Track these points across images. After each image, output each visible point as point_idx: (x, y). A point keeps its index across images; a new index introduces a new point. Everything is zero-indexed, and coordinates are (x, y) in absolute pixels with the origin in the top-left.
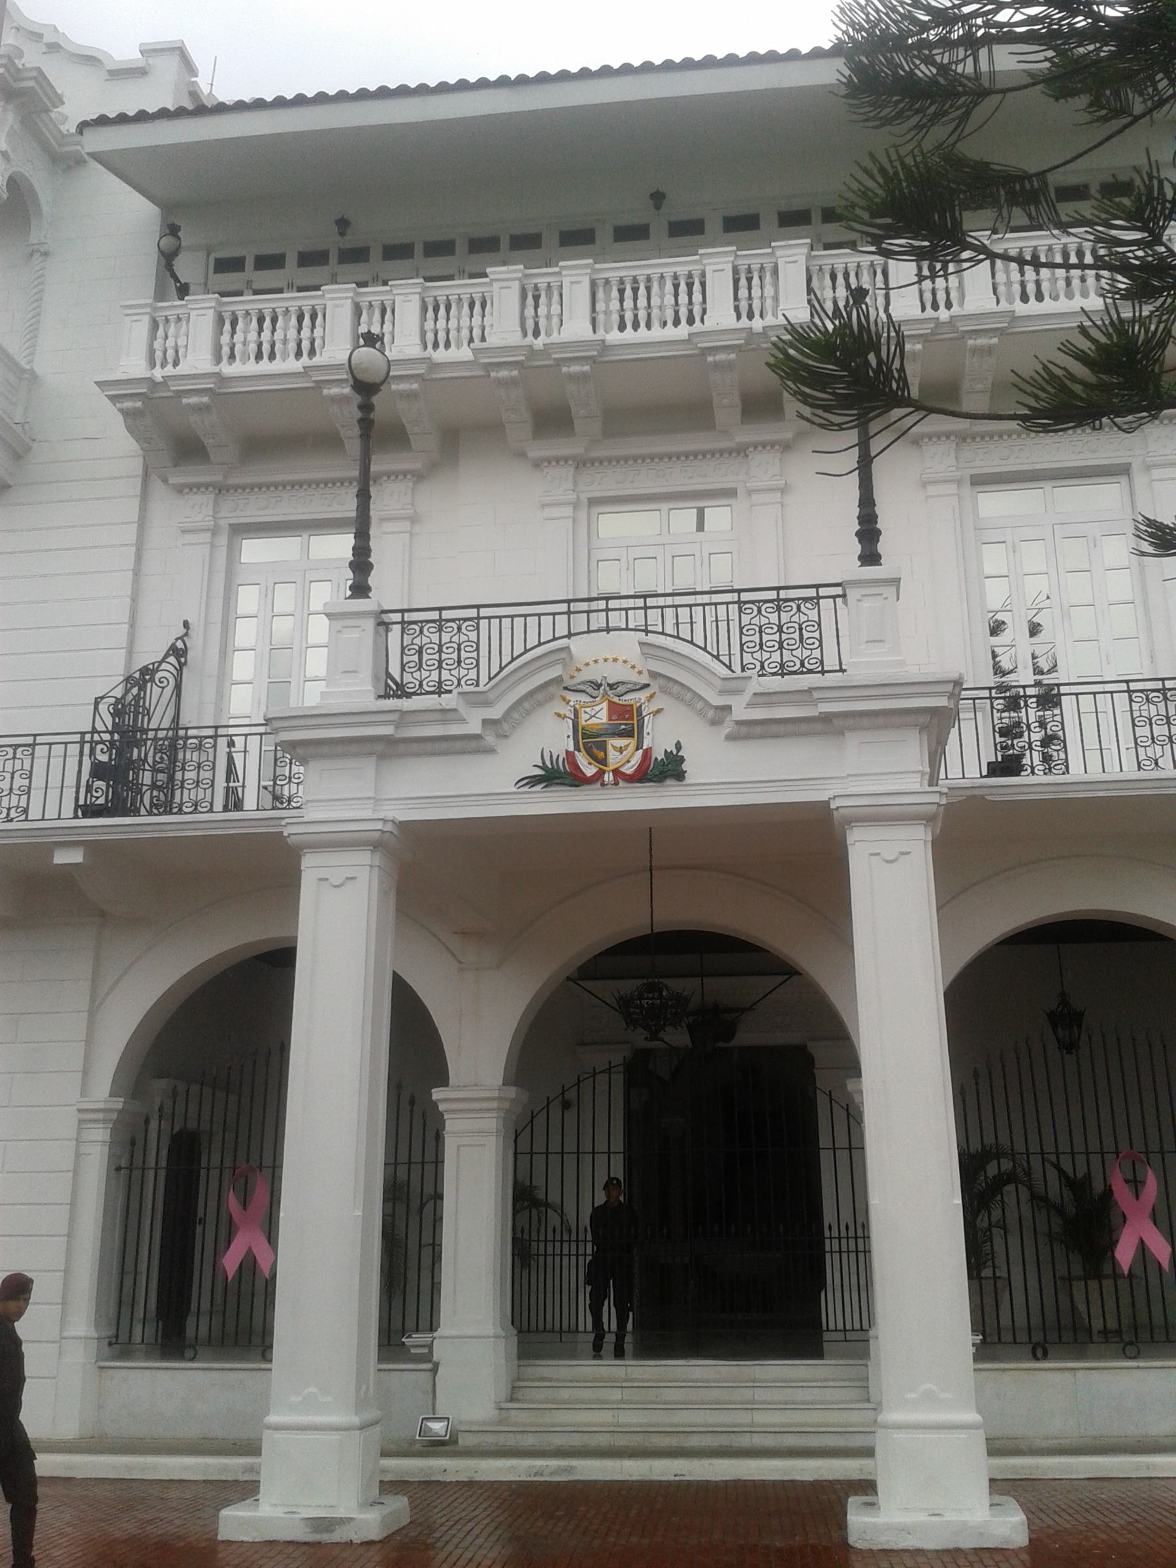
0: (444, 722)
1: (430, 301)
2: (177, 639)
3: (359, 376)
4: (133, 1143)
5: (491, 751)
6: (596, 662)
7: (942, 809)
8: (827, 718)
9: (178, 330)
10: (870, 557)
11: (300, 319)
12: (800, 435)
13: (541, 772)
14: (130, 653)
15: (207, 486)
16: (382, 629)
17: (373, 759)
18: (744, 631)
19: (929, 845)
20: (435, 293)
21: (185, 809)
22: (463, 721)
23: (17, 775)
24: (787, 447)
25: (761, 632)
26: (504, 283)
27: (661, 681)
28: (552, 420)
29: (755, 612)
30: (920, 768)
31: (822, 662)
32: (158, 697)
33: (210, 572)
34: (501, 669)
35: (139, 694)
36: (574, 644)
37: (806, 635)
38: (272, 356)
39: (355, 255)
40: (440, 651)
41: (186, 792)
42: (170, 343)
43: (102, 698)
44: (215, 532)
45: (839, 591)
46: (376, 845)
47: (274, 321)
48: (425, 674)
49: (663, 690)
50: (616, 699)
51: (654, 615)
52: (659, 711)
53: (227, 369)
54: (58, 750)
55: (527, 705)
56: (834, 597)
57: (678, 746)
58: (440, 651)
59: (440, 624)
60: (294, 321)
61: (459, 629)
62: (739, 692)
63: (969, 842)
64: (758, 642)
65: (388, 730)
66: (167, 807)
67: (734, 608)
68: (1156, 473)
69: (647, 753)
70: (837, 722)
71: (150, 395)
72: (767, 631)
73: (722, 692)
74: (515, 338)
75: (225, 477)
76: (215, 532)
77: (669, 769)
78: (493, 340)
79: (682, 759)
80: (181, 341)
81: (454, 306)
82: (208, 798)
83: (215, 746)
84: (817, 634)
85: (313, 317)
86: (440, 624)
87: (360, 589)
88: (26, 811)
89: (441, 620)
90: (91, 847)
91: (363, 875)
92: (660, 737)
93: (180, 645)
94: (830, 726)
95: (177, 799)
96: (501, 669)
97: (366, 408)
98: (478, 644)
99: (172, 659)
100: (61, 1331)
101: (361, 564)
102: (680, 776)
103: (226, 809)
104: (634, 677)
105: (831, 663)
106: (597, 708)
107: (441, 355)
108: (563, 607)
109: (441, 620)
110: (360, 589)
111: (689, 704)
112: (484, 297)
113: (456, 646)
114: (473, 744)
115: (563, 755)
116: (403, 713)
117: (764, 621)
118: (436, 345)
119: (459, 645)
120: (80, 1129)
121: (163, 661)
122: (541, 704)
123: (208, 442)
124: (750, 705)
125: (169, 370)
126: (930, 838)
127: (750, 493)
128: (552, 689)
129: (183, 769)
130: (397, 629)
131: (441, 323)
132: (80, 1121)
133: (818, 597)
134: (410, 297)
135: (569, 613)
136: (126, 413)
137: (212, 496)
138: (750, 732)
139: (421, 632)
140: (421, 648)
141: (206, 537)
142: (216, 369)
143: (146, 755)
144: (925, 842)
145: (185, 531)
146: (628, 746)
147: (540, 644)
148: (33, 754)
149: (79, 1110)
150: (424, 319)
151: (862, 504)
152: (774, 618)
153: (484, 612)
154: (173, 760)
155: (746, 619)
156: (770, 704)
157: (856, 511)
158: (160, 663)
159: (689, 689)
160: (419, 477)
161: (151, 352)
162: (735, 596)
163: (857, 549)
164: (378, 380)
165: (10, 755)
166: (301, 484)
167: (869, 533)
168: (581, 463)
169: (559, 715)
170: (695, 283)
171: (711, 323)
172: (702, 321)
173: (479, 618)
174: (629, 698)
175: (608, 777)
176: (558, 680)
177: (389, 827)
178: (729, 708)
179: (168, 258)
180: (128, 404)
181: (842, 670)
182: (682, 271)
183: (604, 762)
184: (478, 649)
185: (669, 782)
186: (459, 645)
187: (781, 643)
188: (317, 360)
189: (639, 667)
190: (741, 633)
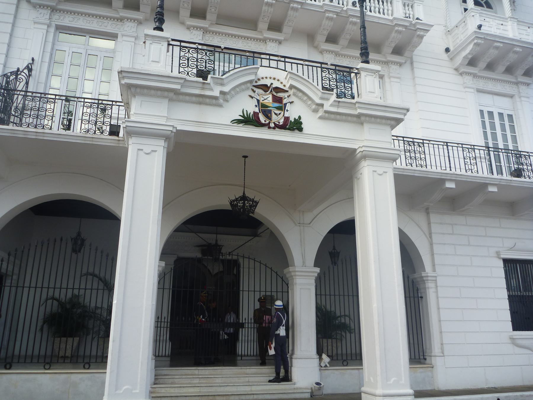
0: (203, 89)
5: (220, 106)
6: (266, 78)
8: (359, 116)
12: (286, 40)
14: (5, 66)
24: (280, 43)
25: (330, 80)
27: (293, 90)
33: (45, 41)
44: (49, 26)
46: (167, 138)
49: (294, 94)
50: (275, 94)
51: (288, 65)
55: (238, 89)
57: (300, 117)
58: (197, 61)
62: (328, 99)
65: (178, 87)
67: (319, 69)
68: (392, 79)
70: (363, 118)
73: (322, 98)
75: (56, 5)
79: (301, 123)
94: (359, 119)
99: (26, 71)
102: (300, 129)
104: (281, 86)
106: (265, 97)
111: (304, 102)
114: (214, 101)
115: (252, 113)
122: (243, 90)
124: (331, 105)
128: (249, 85)
130: (177, 49)
137: (50, 12)
138: (330, 116)
139: (189, 51)
145: (35, 23)
146: (280, 114)
152: (334, 76)
155: (324, 74)
156: (338, 107)
160: (140, 23)
162: (319, 65)
166: (89, 15)
174: (280, 95)
175: (272, 125)
176: (251, 82)
178: (322, 105)
183: (270, 118)
185: (297, 131)
187: (337, 86)
190: (322, 80)
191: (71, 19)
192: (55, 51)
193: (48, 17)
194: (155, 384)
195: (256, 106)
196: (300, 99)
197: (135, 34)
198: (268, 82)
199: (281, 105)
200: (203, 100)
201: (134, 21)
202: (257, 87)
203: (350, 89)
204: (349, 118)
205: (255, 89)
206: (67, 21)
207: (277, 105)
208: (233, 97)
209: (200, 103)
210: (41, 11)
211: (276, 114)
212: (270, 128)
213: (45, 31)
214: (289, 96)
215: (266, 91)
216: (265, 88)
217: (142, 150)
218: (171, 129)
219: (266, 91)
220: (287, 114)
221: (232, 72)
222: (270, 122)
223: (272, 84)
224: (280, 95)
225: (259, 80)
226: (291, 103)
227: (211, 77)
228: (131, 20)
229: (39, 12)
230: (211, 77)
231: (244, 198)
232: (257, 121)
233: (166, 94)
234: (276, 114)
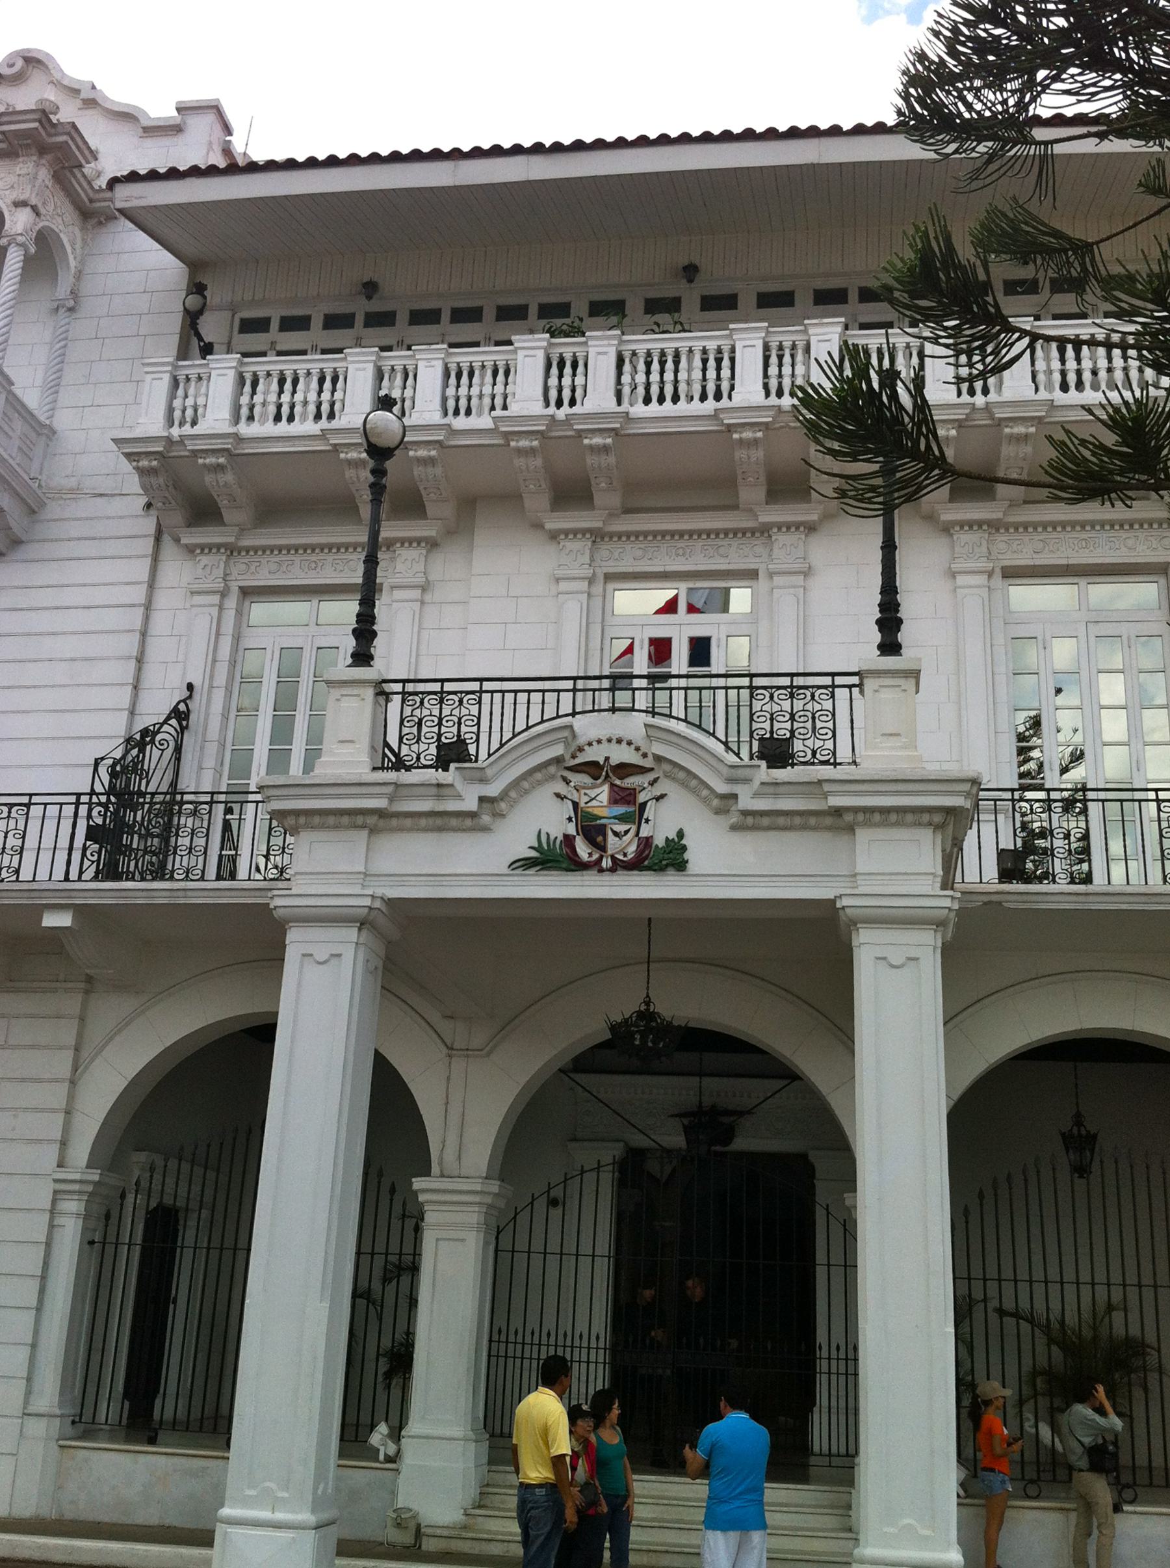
0: (439, 797)
1: (453, 368)
2: (178, 703)
3: (373, 440)
4: (108, 1217)
5: (486, 829)
6: (599, 742)
7: (952, 915)
8: (838, 812)
9: (197, 389)
10: (890, 647)
11: (322, 381)
12: (827, 517)
13: (534, 854)
14: (132, 713)
15: (219, 546)
16: (382, 699)
17: (365, 833)
18: (755, 717)
19: (939, 951)
20: (458, 359)
21: (176, 876)
22: (459, 797)
23: (10, 835)
24: (811, 528)
25: (772, 719)
26: (529, 353)
27: (666, 767)
28: (571, 492)
29: (767, 699)
30: (933, 871)
31: (834, 753)
32: (156, 758)
34: (502, 745)
35: (138, 756)
36: (578, 723)
37: (819, 724)
38: (291, 418)
39: (381, 319)
40: (440, 724)
41: (178, 858)
42: (190, 402)
43: (102, 759)
45: (855, 680)
46: (363, 923)
47: (295, 382)
48: (423, 747)
49: (667, 776)
50: (618, 782)
52: (662, 796)
53: (244, 429)
54: (53, 811)
56: (850, 687)
57: (681, 834)
58: (440, 724)
59: (441, 696)
60: (314, 385)
61: (461, 702)
62: (747, 781)
63: (978, 948)
64: (768, 729)
66: (160, 872)
67: (745, 693)
69: (648, 841)
70: (848, 818)
71: (166, 455)
72: (780, 718)
73: (731, 780)
74: (537, 408)
75: (237, 539)
76: (224, 594)
77: (670, 857)
78: (515, 409)
79: (684, 848)
80: (201, 401)
81: (477, 373)
82: (200, 866)
83: (210, 812)
84: (830, 725)
85: (335, 380)
86: (441, 696)
87: (362, 657)
88: (17, 872)
89: (442, 692)
90: (80, 911)
91: (349, 953)
92: (661, 825)
93: (182, 707)
94: (841, 822)
95: (170, 867)
96: (502, 745)
97: (379, 472)
98: (479, 719)
99: (173, 722)
100: (25, 1408)
101: (365, 631)
103: (219, 878)
105: (844, 754)
107: (461, 422)
108: (569, 684)
109: (442, 692)
110: (362, 657)
111: (694, 791)
112: (507, 365)
113: (456, 720)
114: (468, 822)
115: (560, 838)
116: (397, 785)
117: (776, 708)
118: (456, 412)
119: (460, 719)
120: (54, 1202)
121: (165, 722)
122: (540, 783)
123: (223, 503)
125: (187, 430)
126: (939, 944)
127: (771, 575)
128: (552, 769)
129: (177, 835)
131: (463, 391)
132: (55, 1192)
133: (834, 686)
134: (434, 363)
135: (574, 690)
136: (141, 471)
139: (422, 703)
140: (420, 720)
141: (216, 599)
142: (232, 430)
143: (143, 818)
144: (935, 948)
146: (627, 832)
147: (543, 721)
148: (27, 814)
149: (55, 1181)
150: (446, 385)
151: (883, 592)
152: (786, 705)
153: (487, 686)
154: (168, 826)
156: (776, 795)
157: (878, 598)
158: (162, 725)
159: (696, 777)
160: (432, 544)
161: (170, 410)
163: (877, 637)
164: (392, 446)
165: (5, 814)
167: (890, 621)
168: (597, 536)
169: (558, 795)
170: (725, 359)
171: (738, 399)
172: (730, 397)
173: (481, 691)
175: (606, 863)
176: (558, 760)
177: (378, 904)
178: (735, 797)
179: (192, 318)
180: (144, 463)
181: (854, 763)
182: (712, 345)
183: (602, 848)
184: (478, 724)
185: (671, 871)
186: (460, 719)
188: (335, 424)
189: (643, 750)
190: (752, 719)
191: (274, 567)
192: (241, 653)
193: (220, 572)
194: (480, 1507)
195: (570, 819)
196: (684, 785)
197: (420, 580)
198: (595, 754)
199: (631, 809)
200: (442, 822)
201: (419, 544)
202: (575, 769)
203: (830, 734)
204: (813, 821)
205: (569, 775)
206: (265, 573)
207: (621, 810)
208: (513, 804)
209: (440, 829)
210: (205, 560)
211: (616, 834)
212: (601, 870)
213: (215, 611)
214: (652, 784)
215: (596, 778)
216: (593, 769)
217: (311, 955)
218: (367, 902)
219: (596, 778)
220: (645, 831)
221: (506, 748)
222: (601, 858)
223: (607, 759)
224: (632, 781)
225: (581, 749)
226: (658, 799)
227: (457, 768)
228: (410, 544)
229: (202, 564)
230: (457, 768)
231: (647, 1015)
232: (570, 859)
233: (360, 820)
234: (616, 834)
